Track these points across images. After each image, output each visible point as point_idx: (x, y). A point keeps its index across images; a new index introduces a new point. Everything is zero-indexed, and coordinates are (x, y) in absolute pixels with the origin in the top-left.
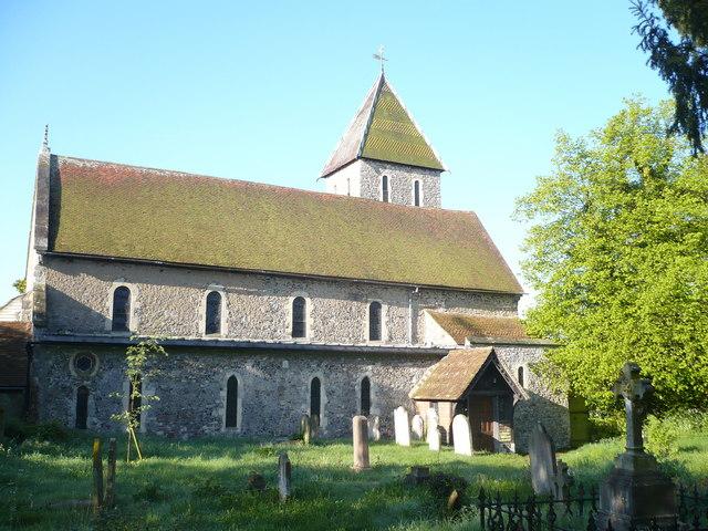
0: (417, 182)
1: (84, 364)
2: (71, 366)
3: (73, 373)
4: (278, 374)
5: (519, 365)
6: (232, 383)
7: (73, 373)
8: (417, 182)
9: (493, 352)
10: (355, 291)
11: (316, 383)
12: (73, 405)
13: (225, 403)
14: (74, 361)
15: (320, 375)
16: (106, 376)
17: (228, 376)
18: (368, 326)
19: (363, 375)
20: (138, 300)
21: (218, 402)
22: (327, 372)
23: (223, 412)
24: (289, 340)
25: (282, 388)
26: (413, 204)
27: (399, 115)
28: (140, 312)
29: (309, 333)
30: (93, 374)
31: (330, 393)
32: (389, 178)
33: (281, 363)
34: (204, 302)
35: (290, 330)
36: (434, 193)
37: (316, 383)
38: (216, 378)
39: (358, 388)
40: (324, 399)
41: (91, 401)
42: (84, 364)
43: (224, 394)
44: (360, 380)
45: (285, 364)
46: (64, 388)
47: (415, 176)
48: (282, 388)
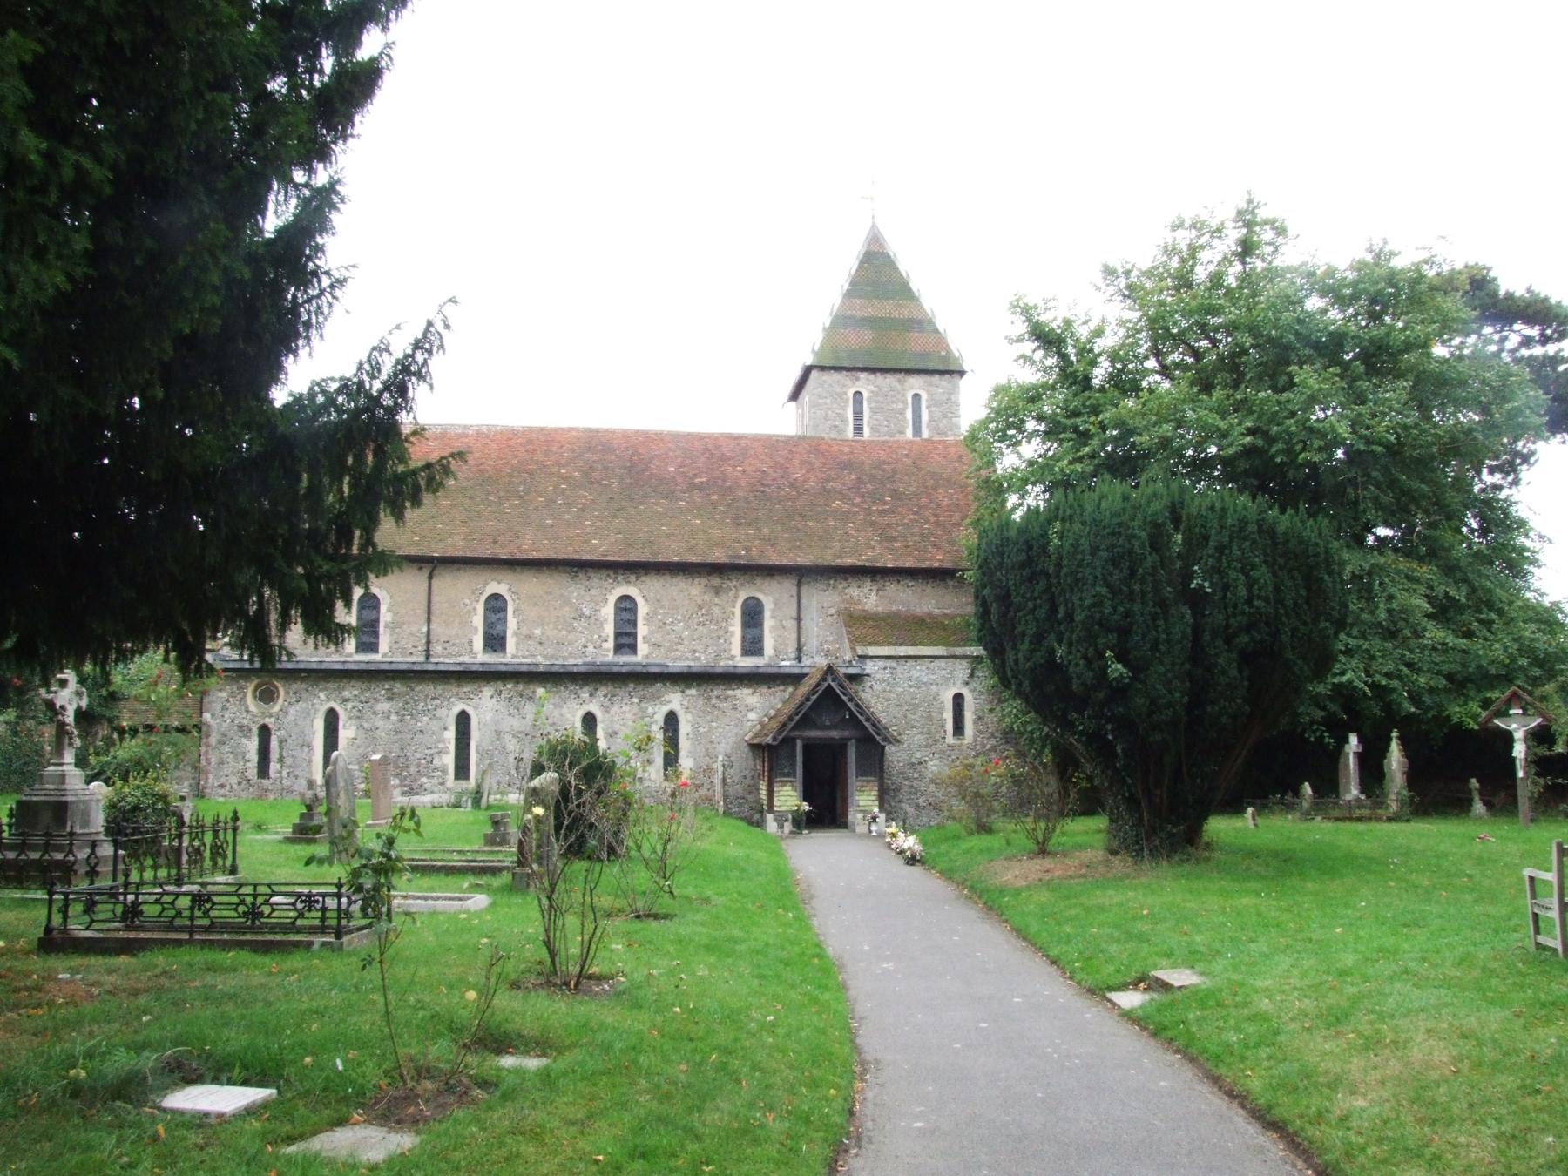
0: (917, 397)
2: (249, 698)
3: (252, 708)
5: (955, 691)
6: (463, 720)
7: (252, 708)
8: (917, 397)
10: (716, 581)
12: (252, 746)
13: (452, 747)
14: (255, 690)
15: (594, 708)
16: (292, 711)
17: (456, 710)
19: (665, 709)
20: (389, 610)
21: (441, 745)
22: (607, 703)
23: (449, 760)
24: (610, 657)
26: (909, 433)
27: (903, 291)
28: (394, 626)
29: (643, 649)
30: (276, 708)
32: (866, 395)
33: (534, 692)
34: (480, 608)
35: (610, 644)
38: (439, 713)
41: (274, 744)
43: (451, 735)
44: (660, 718)
45: (540, 691)
46: (241, 727)
47: (915, 384)
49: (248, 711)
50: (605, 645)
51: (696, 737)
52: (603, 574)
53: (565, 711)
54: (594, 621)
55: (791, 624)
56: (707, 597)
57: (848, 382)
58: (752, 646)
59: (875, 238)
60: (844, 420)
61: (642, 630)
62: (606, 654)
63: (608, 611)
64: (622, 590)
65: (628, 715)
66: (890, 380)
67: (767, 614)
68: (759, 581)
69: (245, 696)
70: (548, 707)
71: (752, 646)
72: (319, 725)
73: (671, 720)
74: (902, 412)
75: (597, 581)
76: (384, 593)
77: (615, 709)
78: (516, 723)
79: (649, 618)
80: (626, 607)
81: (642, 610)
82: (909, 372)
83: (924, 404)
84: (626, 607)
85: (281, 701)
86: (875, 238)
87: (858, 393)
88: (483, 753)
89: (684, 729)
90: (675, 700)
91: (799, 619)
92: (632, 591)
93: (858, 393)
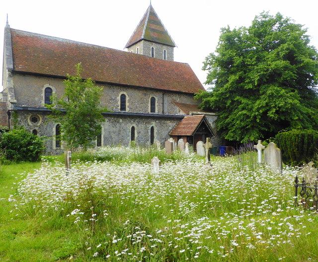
1: (34, 120)
4: (118, 125)
7: (30, 123)
9: (204, 117)
11: (133, 128)
15: (134, 125)
18: (150, 106)
25: (120, 131)
29: (127, 110)
31: (139, 133)
32: (154, 49)
35: (119, 108)
36: (171, 55)
37: (133, 128)
39: (149, 131)
40: (136, 135)
42: (34, 120)
44: (150, 128)
45: (121, 120)
48: (120, 131)
49: (28, 125)
50: (118, 108)
51: (158, 133)
52: (117, 87)
53: (127, 126)
54: (115, 100)
55: (161, 105)
56: (143, 96)
57: (151, 45)
58: (153, 110)
59: (151, 8)
60: (150, 54)
61: (127, 104)
62: (118, 110)
63: (119, 98)
64: (122, 93)
65: (143, 127)
66: (159, 46)
67: (156, 102)
68: (154, 93)
69: (27, 119)
70: (123, 125)
71: (153, 110)
72: (54, 129)
73: (152, 129)
74: (162, 54)
75: (116, 88)
76: (54, 88)
77: (140, 126)
78: (114, 129)
79: (129, 101)
80: (123, 98)
81: (127, 99)
82: (164, 44)
83: (166, 53)
84: (123, 98)
85: (40, 121)
86: (151, 8)
87: (153, 48)
88: (105, 138)
89: (155, 131)
90: (154, 124)
91: (163, 104)
92: (125, 93)
93: (153, 48)
